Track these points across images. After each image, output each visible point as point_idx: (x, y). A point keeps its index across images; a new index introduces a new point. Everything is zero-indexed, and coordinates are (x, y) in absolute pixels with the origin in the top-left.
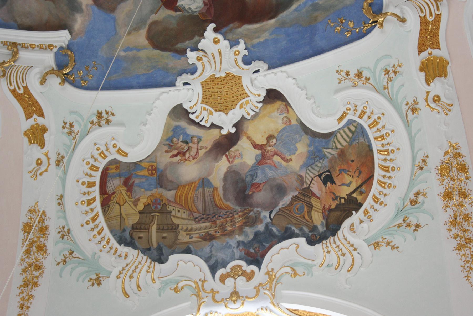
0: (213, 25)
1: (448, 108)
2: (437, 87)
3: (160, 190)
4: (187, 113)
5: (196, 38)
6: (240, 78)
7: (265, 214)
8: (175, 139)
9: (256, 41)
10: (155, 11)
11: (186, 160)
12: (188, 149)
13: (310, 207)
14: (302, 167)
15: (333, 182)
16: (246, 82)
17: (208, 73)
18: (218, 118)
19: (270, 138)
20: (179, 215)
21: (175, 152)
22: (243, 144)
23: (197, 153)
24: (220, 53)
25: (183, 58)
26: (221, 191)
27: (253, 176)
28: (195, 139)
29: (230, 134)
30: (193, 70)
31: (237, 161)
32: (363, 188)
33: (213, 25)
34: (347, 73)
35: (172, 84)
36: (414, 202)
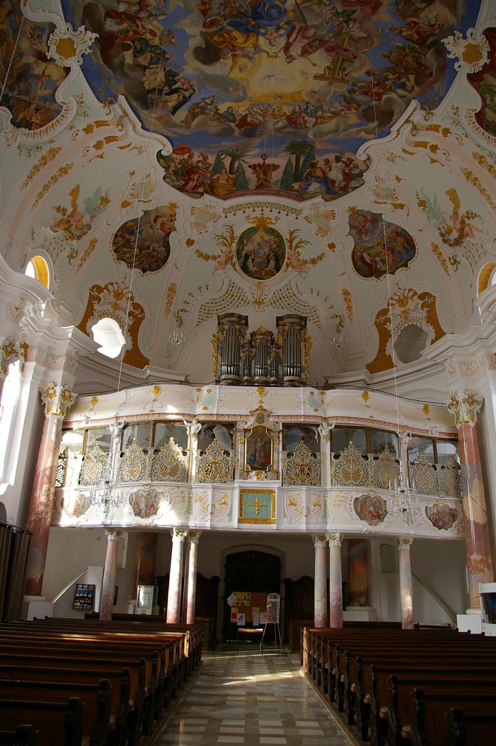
0: (98, 36)
1: (74, 140)
2: (82, 134)
3: (12, 33)
4: (53, 32)
5: (91, 29)
6: (75, 55)
7: (16, 92)
8: (38, 30)
9: (92, 57)
10: (103, 6)
11: (29, 39)
12: (35, 39)
13: (24, 110)
14: (39, 96)
15: (36, 113)
16: (73, 58)
17: (74, 39)
18: (53, 48)
19: (49, 76)
20: (3, 50)
21: (32, 33)
22: (43, 65)
23: (34, 44)
24: (85, 42)
25: (80, 24)
26: (20, 65)
27: (30, 77)
28: (41, 41)
29: (47, 56)
30: (75, 30)
31: (35, 66)
32: (37, 126)
33: (98, 36)
34: (82, 98)
35: (66, 20)
36: (37, 148)
